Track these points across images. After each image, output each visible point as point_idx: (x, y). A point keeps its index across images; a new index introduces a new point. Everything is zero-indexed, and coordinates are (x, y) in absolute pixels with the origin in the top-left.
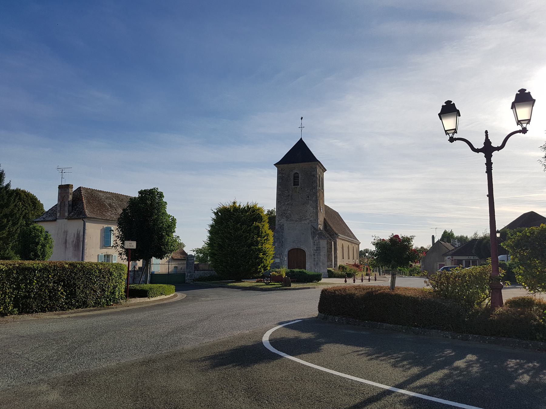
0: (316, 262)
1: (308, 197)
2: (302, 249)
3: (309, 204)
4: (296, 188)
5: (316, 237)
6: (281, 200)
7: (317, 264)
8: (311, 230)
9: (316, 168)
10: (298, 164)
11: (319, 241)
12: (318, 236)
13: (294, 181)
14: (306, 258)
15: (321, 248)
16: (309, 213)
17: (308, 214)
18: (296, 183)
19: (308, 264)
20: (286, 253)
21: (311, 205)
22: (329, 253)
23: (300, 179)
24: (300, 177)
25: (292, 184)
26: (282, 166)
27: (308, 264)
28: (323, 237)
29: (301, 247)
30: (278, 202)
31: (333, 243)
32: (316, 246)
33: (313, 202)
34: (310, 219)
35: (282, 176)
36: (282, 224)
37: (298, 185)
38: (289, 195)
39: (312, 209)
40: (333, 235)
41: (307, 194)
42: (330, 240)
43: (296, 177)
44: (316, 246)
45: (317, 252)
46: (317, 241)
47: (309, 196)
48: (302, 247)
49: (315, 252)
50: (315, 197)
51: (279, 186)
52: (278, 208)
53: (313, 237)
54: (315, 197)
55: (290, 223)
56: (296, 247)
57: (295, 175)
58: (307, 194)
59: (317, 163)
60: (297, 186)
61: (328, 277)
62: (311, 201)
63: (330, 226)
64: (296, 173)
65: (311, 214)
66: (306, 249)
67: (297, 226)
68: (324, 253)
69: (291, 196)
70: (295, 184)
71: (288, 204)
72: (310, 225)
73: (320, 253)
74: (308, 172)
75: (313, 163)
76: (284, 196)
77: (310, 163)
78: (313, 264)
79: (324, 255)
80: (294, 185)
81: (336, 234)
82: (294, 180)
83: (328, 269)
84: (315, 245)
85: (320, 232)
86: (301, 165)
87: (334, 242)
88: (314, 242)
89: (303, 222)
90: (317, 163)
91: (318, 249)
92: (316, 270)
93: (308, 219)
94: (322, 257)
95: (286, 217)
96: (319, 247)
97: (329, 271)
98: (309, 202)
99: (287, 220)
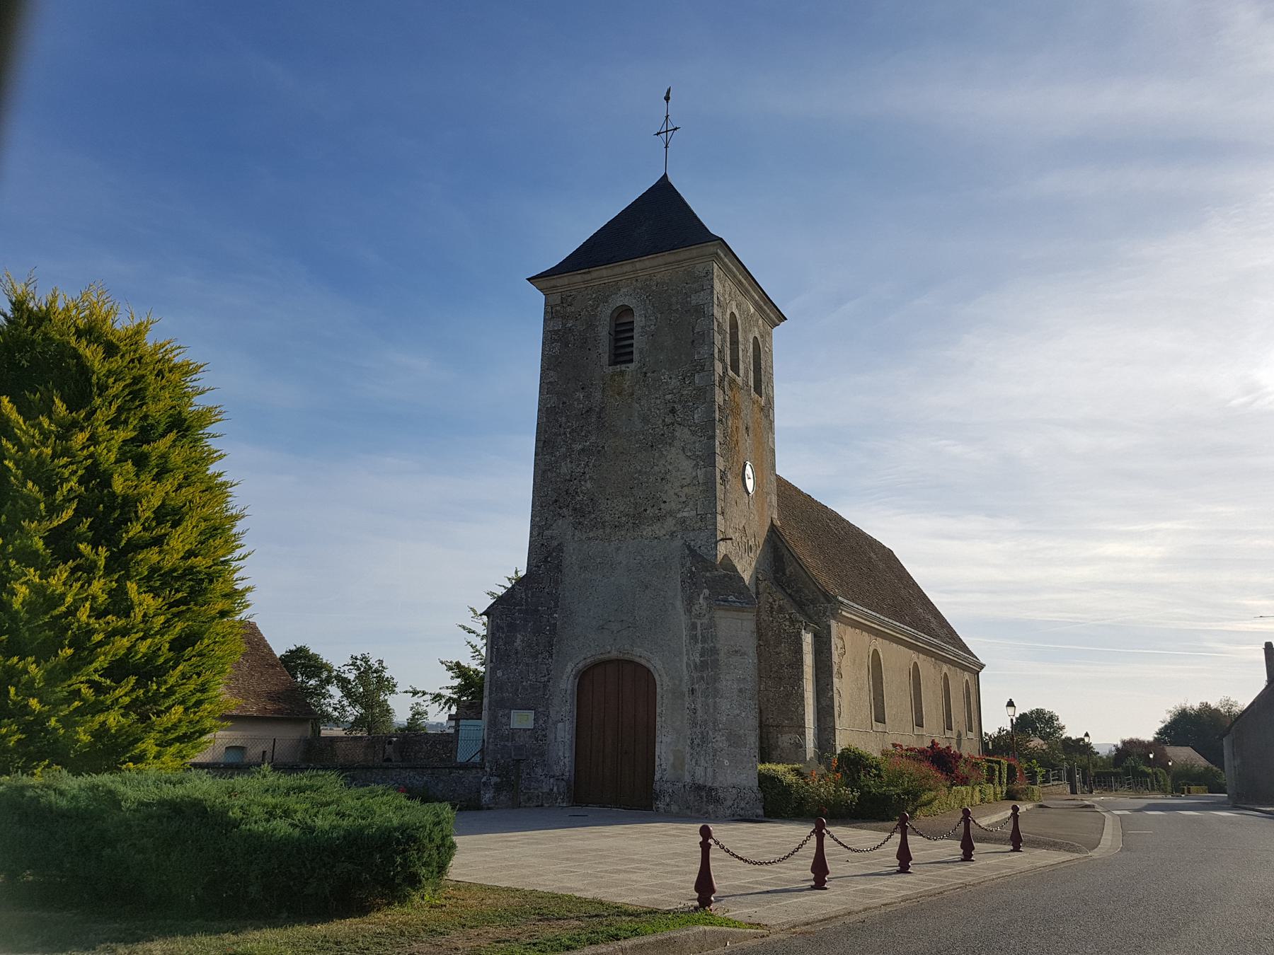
0: (698, 730)
1: (673, 411)
2: (637, 660)
3: (676, 443)
4: (622, 373)
5: (701, 601)
6: (555, 434)
7: (704, 739)
8: (683, 566)
9: (709, 274)
10: (627, 267)
11: (711, 618)
12: (706, 591)
13: (617, 348)
14: (658, 711)
15: (722, 654)
16: (677, 484)
17: (671, 492)
18: (621, 353)
19: (665, 739)
20: (566, 683)
21: (683, 449)
22: (789, 688)
23: (636, 334)
24: (639, 321)
25: (605, 358)
26: (563, 280)
27: (665, 739)
28: (731, 598)
29: (638, 651)
30: (541, 444)
31: (808, 639)
32: (700, 645)
33: (693, 433)
34: (679, 516)
35: (564, 325)
36: (555, 543)
37: (631, 361)
38: (589, 410)
39: (687, 465)
40: (812, 602)
41: (669, 397)
42: (793, 622)
43: (622, 329)
44: (700, 645)
45: (702, 678)
46: (705, 621)
47: (678, 407)
48: (640, 654)
49: (695, 675)
50: (703, 407)
51: (552, 373)
52: (544, 472)
53: (690, 601)
54: (703, 407)
55: (591, 535)
56: (614, 654)
57: (622, 321)
58: (669, 397)
59: (712, 249)
60: (623, 367)
61: (761, 812)
62: (686, 430)
63: (797, 560)
64: (627, 310)
65: (686, 490)
66: (656, 664)
67: (618, 549)
68: (739, 680)
69: (600, 413)
70: (619, 359)
71: (583, 450)
72: (678, 542)
73: (716, 680)
74: (674, 299)
75: (694, 251)
76: (567, 416)
77: (683, 254)
78: (689, 742)
79: (740, 691)
80: (614, 363)
81: (829, 598)
82: (617, 340)
83: (760, 767)
84: (696, 642)
85: (725, 576)
86: (646, 265)
87: (816, 636)
88: (694, 626)
89: (647, 531)
90: (710, 248)
91: (708, 664)
92: (699, 772)
93: (671, 513)
94: (724, 705)
95: (575, 509)
96: (714, 651)
97: (766, 781)
98: (677, 434)
99: (577, 525)
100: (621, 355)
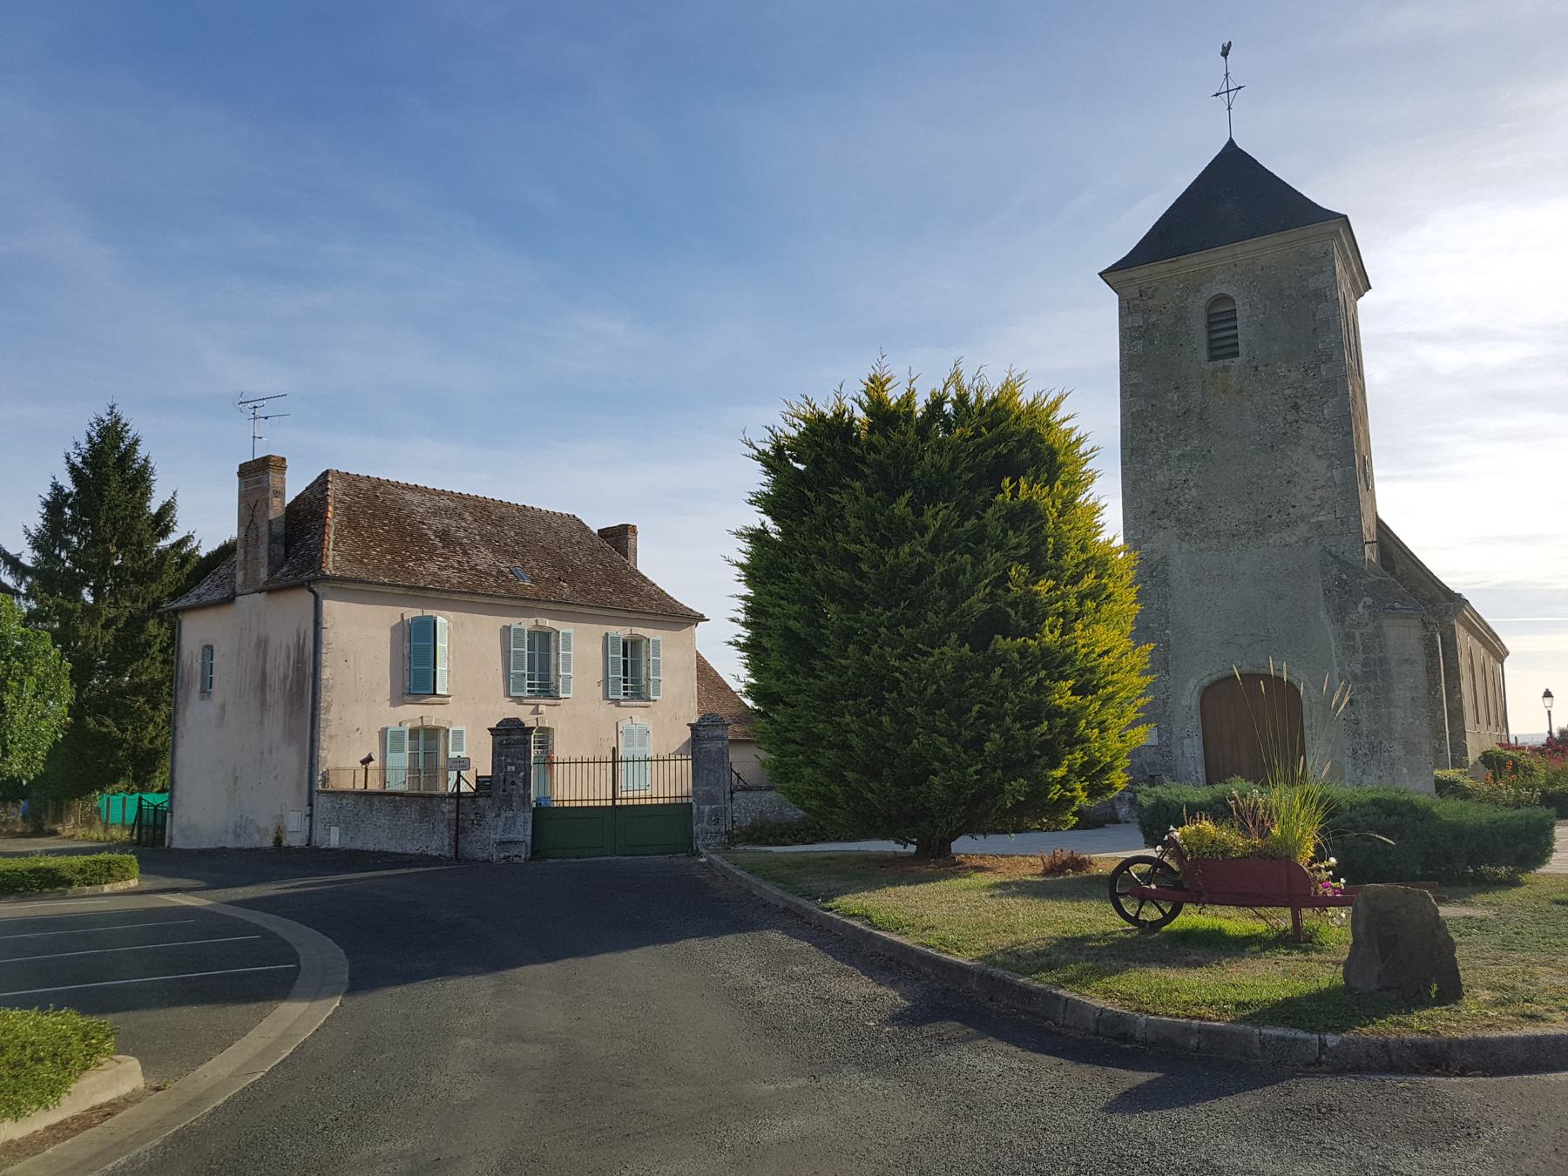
1: (1296, 407)
5: (1360, 609)
6: (1146, 440)
7: (1375, 749)
9: (1328, 256)
10: (1223, 253)
12: (1369, 600)
13: (1211, 341)
14: (1306, 723)
18: (1222, 346)
21: (1313, 448)
23: (1241, 323)
25: (1203, 354)
26: (1141, 272)
28: (1397, 605)
34: (1313, 520)
36: (1157, 557)
37: (1237, 354)
41: (1289, 392)
43: (1220, 319)
44: (1361, 656)
47: (1301, 402)
51: (1135, 374)
52: (1135, 482)
53: (1339, 613)
55: (1203, 546)
57: (1213, 312)
58: (1289, 392)
60: (1227, 362)
62: (1314, 427)
64: (1223, 298)
75: (1310, 230)
77: (1294, 234)
79: (1413, 699)
80: (1213, 358)
82: (1211, 332)
83: (1436, 772)
84: (1354, 650)
88: (1350, 637)
89: (1274, 539)
93: (1303, 518)
96: (1383, 661)
100: (1217, 348)
